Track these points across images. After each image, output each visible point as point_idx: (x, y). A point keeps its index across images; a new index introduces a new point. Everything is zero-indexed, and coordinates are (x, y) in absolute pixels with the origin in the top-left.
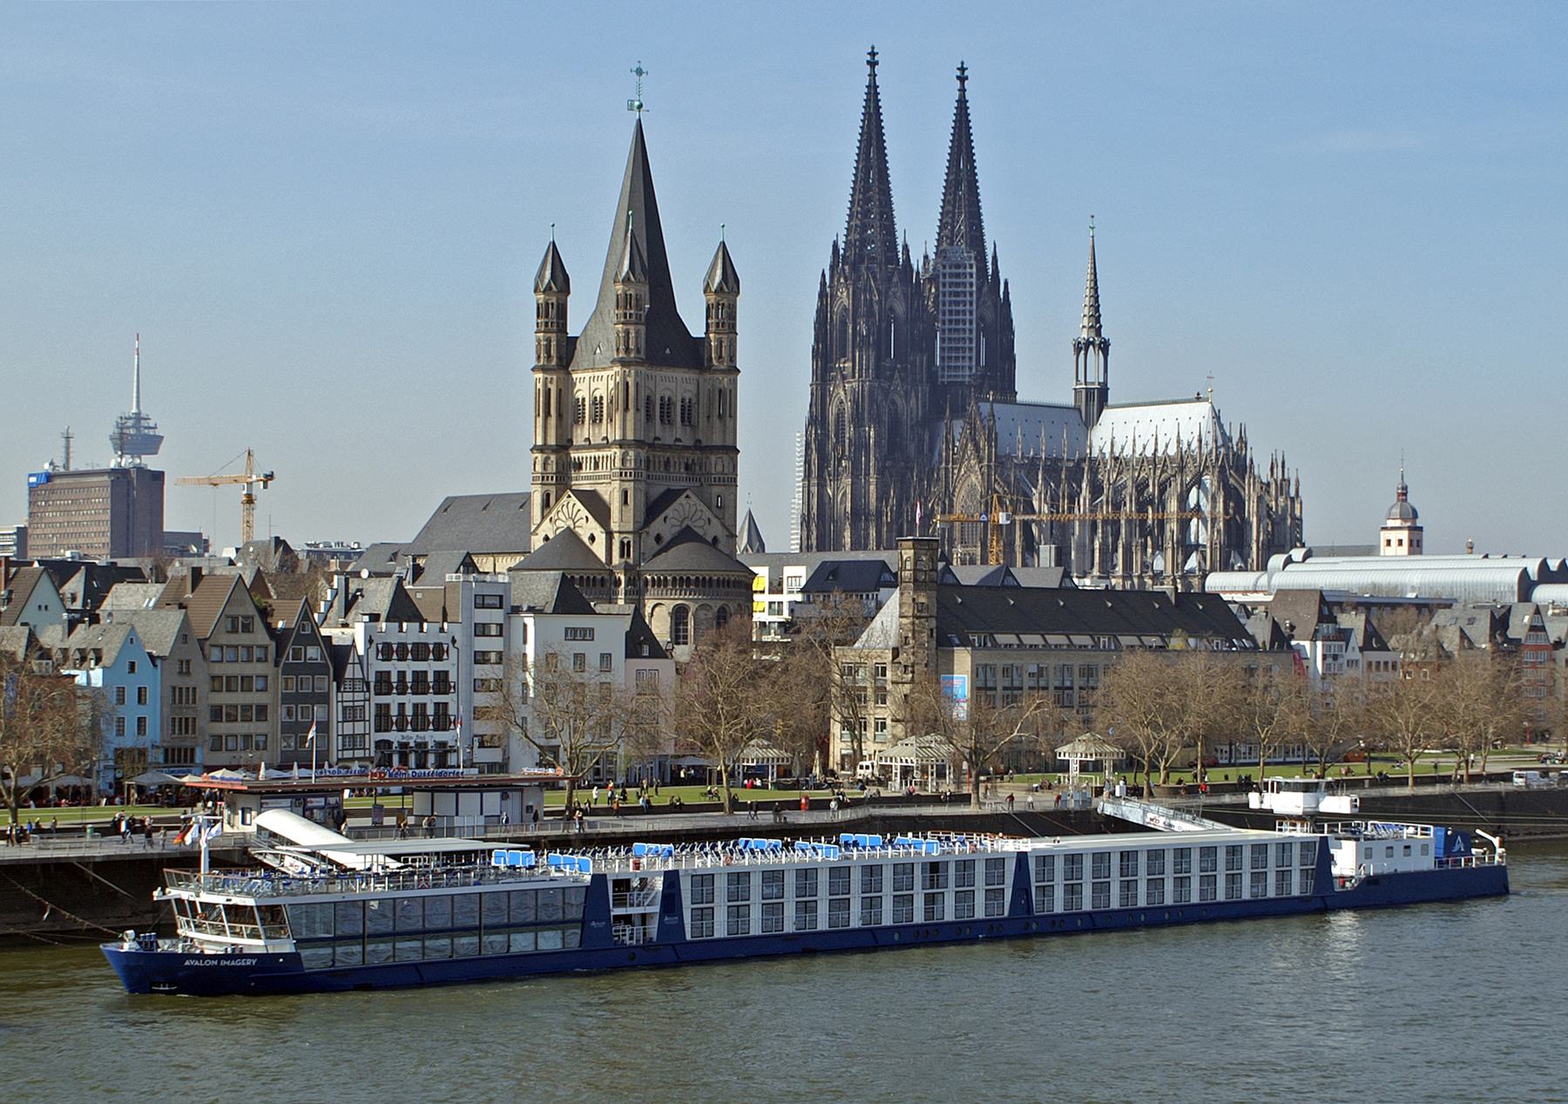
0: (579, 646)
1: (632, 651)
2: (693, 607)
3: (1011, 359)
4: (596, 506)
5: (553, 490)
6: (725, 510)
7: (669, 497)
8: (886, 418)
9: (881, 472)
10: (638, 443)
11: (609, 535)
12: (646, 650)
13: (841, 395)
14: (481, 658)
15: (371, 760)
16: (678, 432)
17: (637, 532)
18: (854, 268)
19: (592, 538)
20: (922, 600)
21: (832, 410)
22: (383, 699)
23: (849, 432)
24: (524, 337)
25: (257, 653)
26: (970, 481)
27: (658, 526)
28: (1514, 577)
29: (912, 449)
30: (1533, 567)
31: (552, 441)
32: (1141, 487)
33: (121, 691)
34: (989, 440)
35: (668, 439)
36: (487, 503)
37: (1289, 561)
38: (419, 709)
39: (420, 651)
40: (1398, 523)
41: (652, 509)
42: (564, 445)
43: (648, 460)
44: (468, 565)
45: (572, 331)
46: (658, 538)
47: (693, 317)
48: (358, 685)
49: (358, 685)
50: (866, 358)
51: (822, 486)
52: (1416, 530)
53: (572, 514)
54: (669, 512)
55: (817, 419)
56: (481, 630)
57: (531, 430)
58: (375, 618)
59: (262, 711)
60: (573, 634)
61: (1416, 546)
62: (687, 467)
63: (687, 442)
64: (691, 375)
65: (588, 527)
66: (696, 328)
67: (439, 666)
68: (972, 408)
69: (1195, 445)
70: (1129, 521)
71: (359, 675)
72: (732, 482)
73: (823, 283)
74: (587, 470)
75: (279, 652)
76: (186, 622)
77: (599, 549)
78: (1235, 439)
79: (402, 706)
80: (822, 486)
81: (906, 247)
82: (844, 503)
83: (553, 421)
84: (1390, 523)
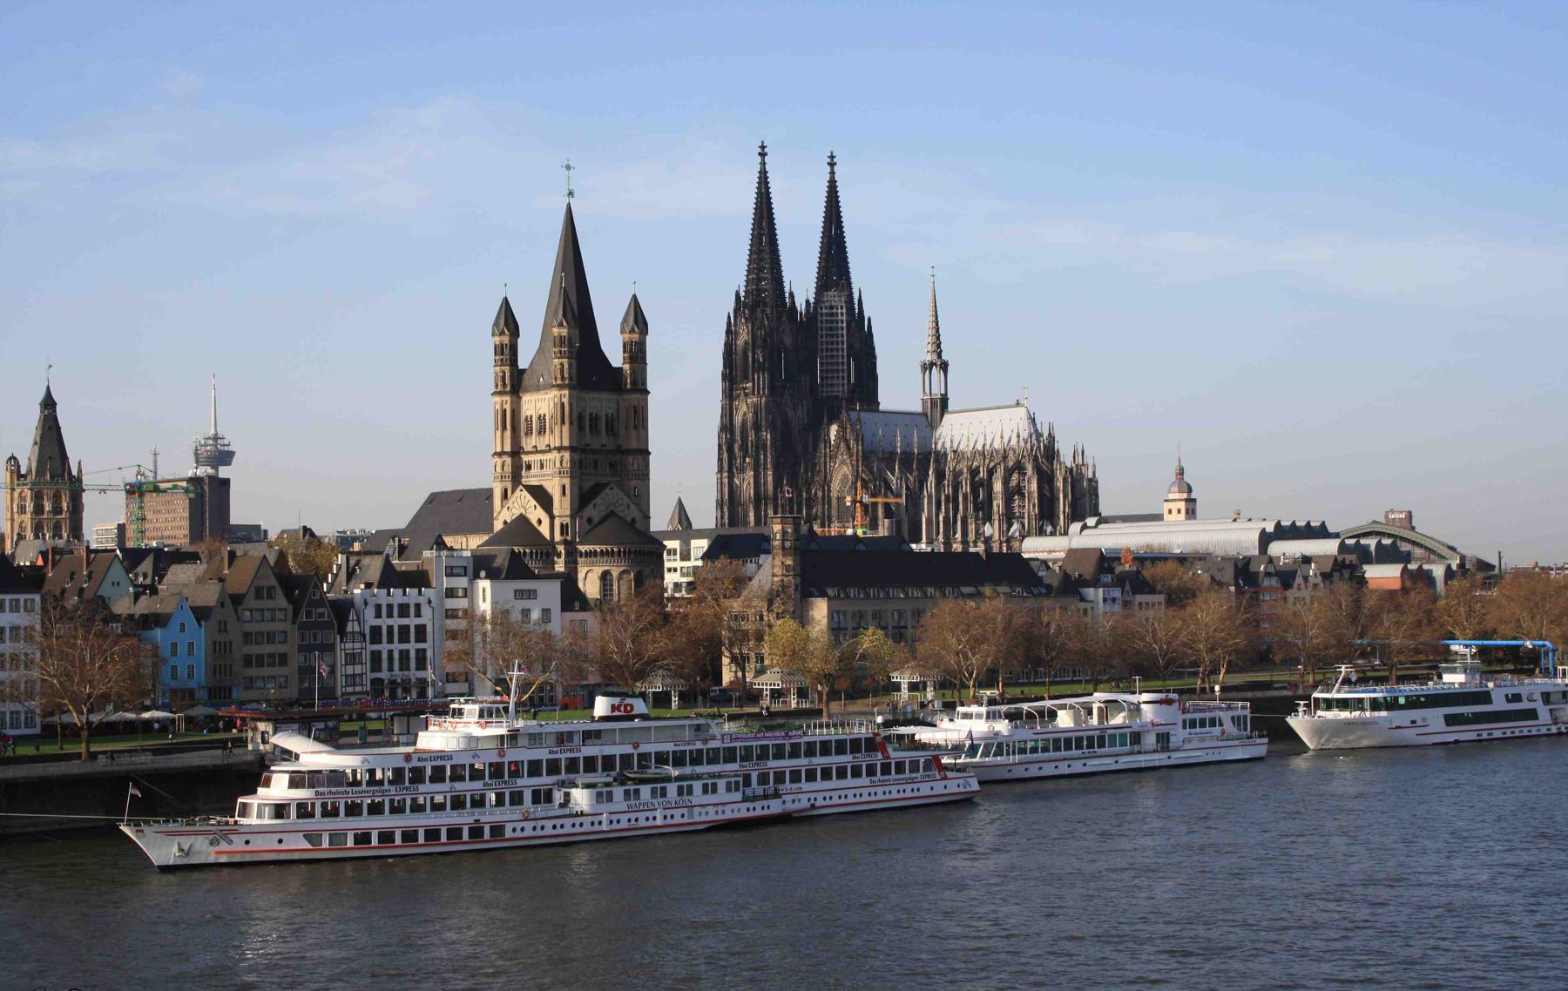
0: (525, 604)
1: (567, 606)
2: (615, 572)
3: (875, 378)
4: (541, 496)
5: (509, 486)
6: (641, 500)
7: (598, 489)
8: (779, 424)
9: (776, 467)
10: (572, 449)
11: (552, 518)
12: (577, 605)
13: (743, 409)
14: (451, 614)
15: (367, 693)
17: (573, 517)
18: (753, 311)
19: (540, 522)
20: (789, 562)
21: (738, 419)
22: (376, 647)
23: (752, 436)
24: (487, 370)
25: (279, 615)
26: (841, 473)
27: (589, 511)
28: (1256, 536)
29: (799, 448)
30: (1270, 528)
31: (508, 448)
32: (974, 472)
33: (174, 645)
34: (857, 440)
35: (595, 446)
36: (461, 496)
37: (1085, 527)
38: (404, 655)
39: (404, 610)
40: (1177, 496)
41: (583, 498)
42: (516, 453)
43: (581, 462)
44: (441, 545)
45: (523, 363)
46: (590, 520)
47: (613, 350)
48: (357, 637)
49: (357, 637)
50: (763, 379)
52: (1191, 501)
53: (523, 504)
54: (598, 500)
55: (727, 427)
56: (451, 593)
57: (491, 439)
58: (368, 585)
59: (283, 660)
60: (520, 594)
61: (1191, 513)
62: (611, 465)
63: (611, 447)
64: (614, 397)
65: (536, 514)
67: (418, 621)
68: (844, 416)
69: (1014, 442)
70: (965, 497)
71: (357, 629)
72: (645, 476)
73: (729, 323)
74: (533, 471)
75: (296, 614)
76: (223, 591)
77: (544, 530)
78: (1046, 435)
79: (390, 652)
80: (731, 478)
81: (791, 294)
83: (508, 433)
84: (1171, 496)
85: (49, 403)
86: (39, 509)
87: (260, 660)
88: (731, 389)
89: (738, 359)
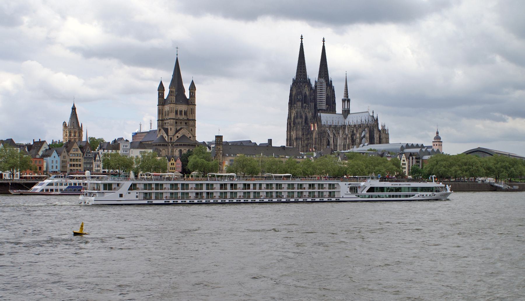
8: (304, 117)
16: (183, 117)
21: (293, 116)
27: (177, 135)
35: (181, 118)
37: (364, 145)
47: (187, 94)
51: (290, 133)
54: (180, 132)
55: (289, 118)
59: (80, 165)
62: (186, 123)
63: (186, 118)
65: (165, 135)
66: (188, 97)
72: (194, 126)
75: (83, 155)
77: (166, 139)
82: (294, 136)
85: (74, 109)
86: (70, 135)
87: (74, 165)
88: (291, 107)
89: (293, 97)
